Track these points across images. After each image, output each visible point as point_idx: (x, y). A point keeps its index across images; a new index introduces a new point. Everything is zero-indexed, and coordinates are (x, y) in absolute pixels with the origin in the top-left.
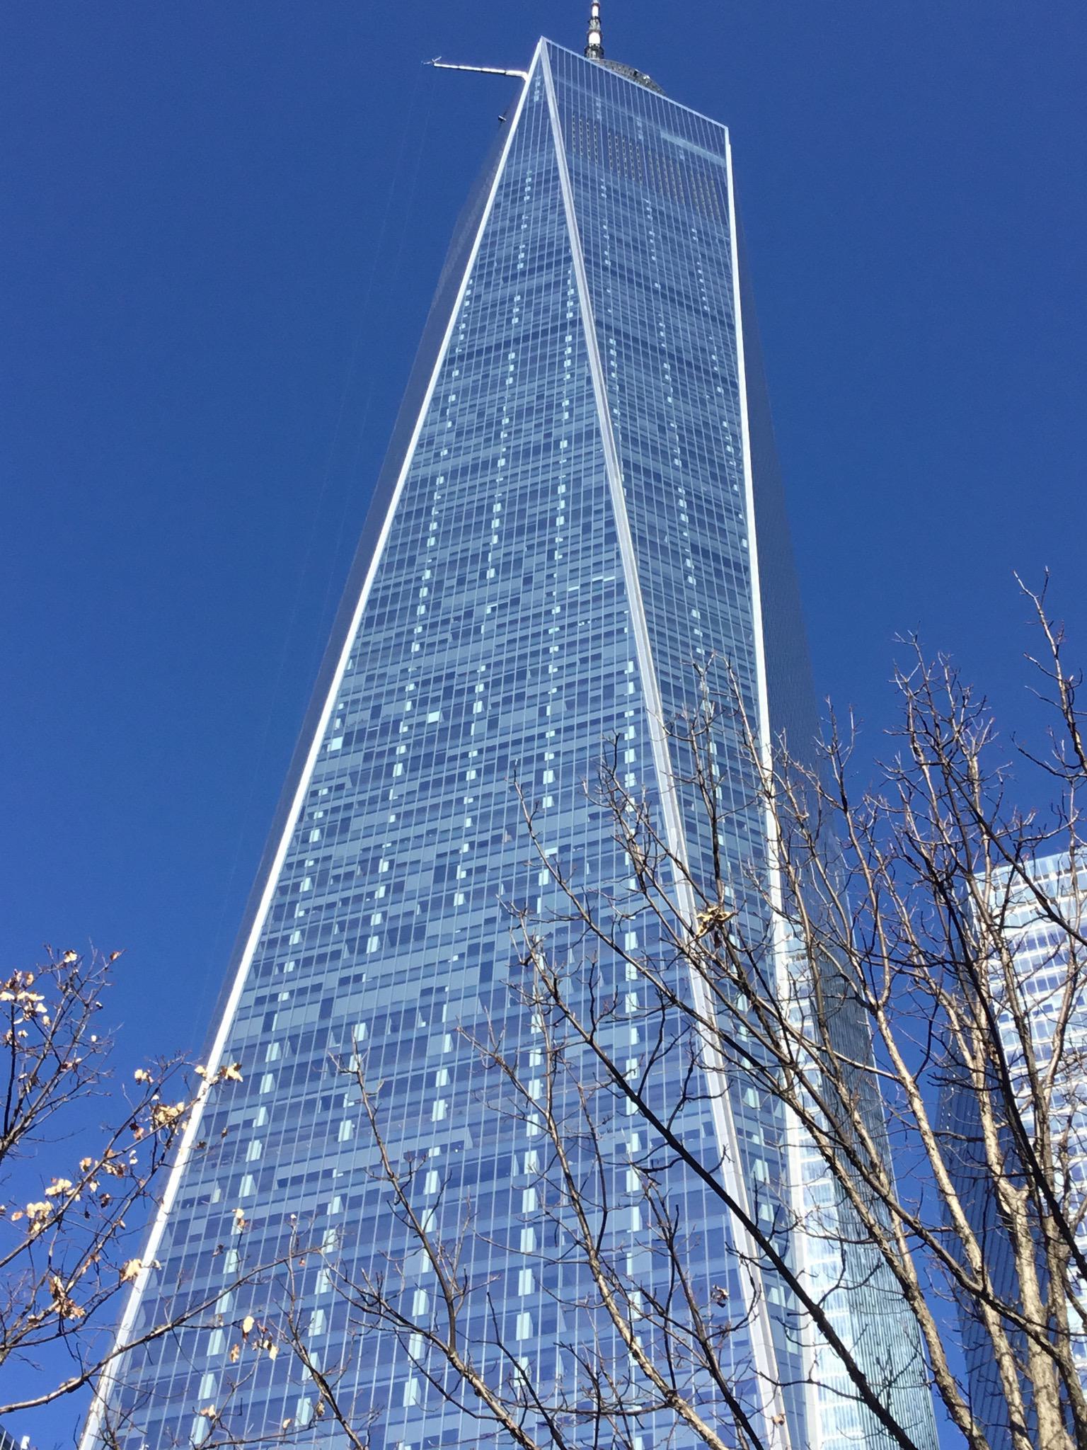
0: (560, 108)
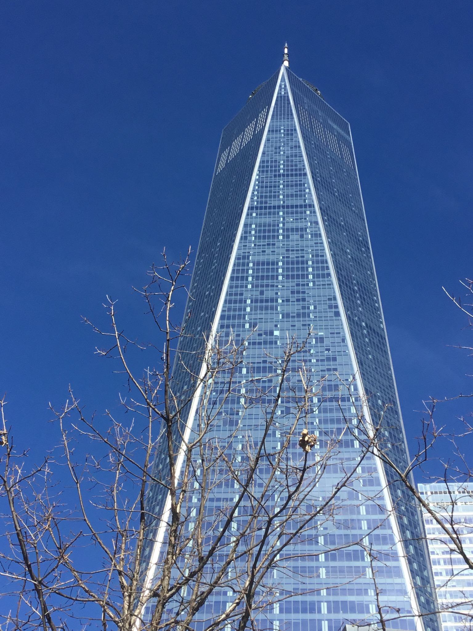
0: (294, 100)
